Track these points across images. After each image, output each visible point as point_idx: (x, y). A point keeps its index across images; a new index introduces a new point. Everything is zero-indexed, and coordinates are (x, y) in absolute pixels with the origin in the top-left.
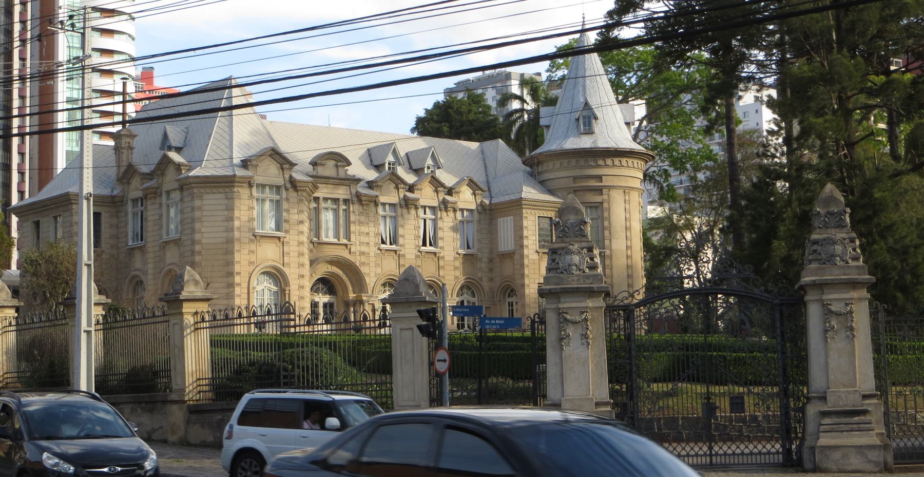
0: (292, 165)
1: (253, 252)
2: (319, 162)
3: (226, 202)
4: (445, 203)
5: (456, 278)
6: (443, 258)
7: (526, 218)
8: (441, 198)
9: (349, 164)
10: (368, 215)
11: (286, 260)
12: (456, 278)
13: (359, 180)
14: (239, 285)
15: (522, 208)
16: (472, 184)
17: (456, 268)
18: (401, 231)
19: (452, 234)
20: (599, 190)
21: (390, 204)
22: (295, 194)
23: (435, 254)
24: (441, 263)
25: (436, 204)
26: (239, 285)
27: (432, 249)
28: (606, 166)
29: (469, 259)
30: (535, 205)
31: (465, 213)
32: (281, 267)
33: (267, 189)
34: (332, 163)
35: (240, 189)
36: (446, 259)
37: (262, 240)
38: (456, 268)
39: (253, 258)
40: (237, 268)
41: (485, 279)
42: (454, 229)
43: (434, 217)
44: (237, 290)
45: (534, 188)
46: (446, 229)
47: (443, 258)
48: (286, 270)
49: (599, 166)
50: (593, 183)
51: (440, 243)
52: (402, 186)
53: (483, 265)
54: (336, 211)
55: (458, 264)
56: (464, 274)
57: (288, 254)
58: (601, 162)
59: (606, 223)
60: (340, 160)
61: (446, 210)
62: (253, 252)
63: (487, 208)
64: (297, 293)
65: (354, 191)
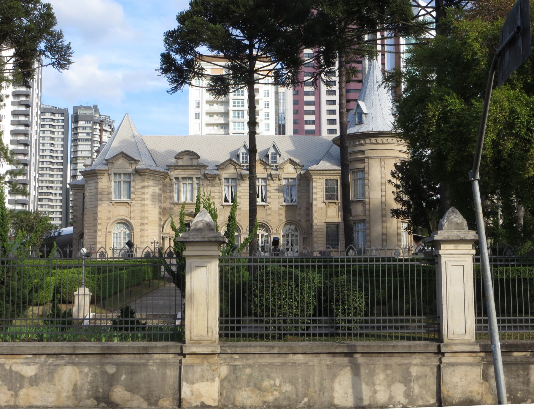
0: (136, 161)
1: (109, 212)
2: (178, 157)
3: (96, 184)
4: (271, 175)
5: (280, 220)
6: (270, 208)
7: (316, 181)
8: (269, 173)
9: (199, 157)
10: (213, 186)
11: (132, 215)
12: (280, 220)
13: (205, 166)
14: (100, 230)
15: (312, 176)
16: (292, 162)
17: (280, 215)
18: (238, 194)
19: (277, 194)
20: (362, 160)
21: (232, 179)
22: (140, 177)
23: (264, 206)
24: (269, 212)
25: (266, 177)
26: (100, 230)
27: (264, 203)
28: (366, 144)
29: (289, 208)
30: (321, 173)
31: (290, 180)
32: (129, 219)
33: (122, 175)
34: (189, 157)
35: (102, 177)
36: (272, 209)
37: (116, 204)
38: (280, 215)
39: (110, 215)
40: (99, 221)
41: (302, 220)
42: (280, 190)
43: (265, 184)
44: (99, 233)
45: (329, 162)
46: (272, 191)
47: (270, 208)
48: (132, 221)
49: (361, 145)
50: (360, 156)
51: (268, 200)
52: (238, 167)
53: (302, 212)
54: (192, 184)
55: (283, 212)
56: (286, 217)
57: (134, 211)
58: (363, 142)
59: (367, 181)
60: (193, 155)
61: (272, 179)
62: (109, 212)
63: (304, 176)
64: (140, 234)
65: (203, 173)
